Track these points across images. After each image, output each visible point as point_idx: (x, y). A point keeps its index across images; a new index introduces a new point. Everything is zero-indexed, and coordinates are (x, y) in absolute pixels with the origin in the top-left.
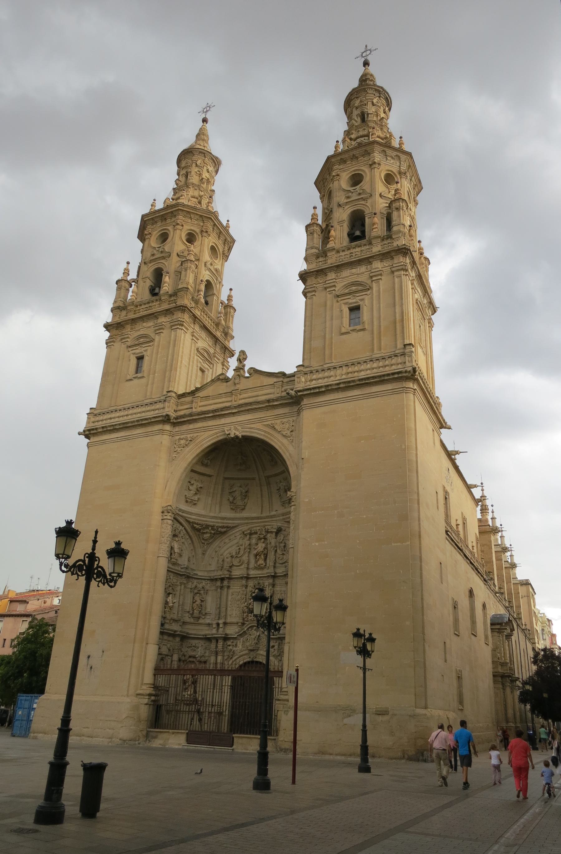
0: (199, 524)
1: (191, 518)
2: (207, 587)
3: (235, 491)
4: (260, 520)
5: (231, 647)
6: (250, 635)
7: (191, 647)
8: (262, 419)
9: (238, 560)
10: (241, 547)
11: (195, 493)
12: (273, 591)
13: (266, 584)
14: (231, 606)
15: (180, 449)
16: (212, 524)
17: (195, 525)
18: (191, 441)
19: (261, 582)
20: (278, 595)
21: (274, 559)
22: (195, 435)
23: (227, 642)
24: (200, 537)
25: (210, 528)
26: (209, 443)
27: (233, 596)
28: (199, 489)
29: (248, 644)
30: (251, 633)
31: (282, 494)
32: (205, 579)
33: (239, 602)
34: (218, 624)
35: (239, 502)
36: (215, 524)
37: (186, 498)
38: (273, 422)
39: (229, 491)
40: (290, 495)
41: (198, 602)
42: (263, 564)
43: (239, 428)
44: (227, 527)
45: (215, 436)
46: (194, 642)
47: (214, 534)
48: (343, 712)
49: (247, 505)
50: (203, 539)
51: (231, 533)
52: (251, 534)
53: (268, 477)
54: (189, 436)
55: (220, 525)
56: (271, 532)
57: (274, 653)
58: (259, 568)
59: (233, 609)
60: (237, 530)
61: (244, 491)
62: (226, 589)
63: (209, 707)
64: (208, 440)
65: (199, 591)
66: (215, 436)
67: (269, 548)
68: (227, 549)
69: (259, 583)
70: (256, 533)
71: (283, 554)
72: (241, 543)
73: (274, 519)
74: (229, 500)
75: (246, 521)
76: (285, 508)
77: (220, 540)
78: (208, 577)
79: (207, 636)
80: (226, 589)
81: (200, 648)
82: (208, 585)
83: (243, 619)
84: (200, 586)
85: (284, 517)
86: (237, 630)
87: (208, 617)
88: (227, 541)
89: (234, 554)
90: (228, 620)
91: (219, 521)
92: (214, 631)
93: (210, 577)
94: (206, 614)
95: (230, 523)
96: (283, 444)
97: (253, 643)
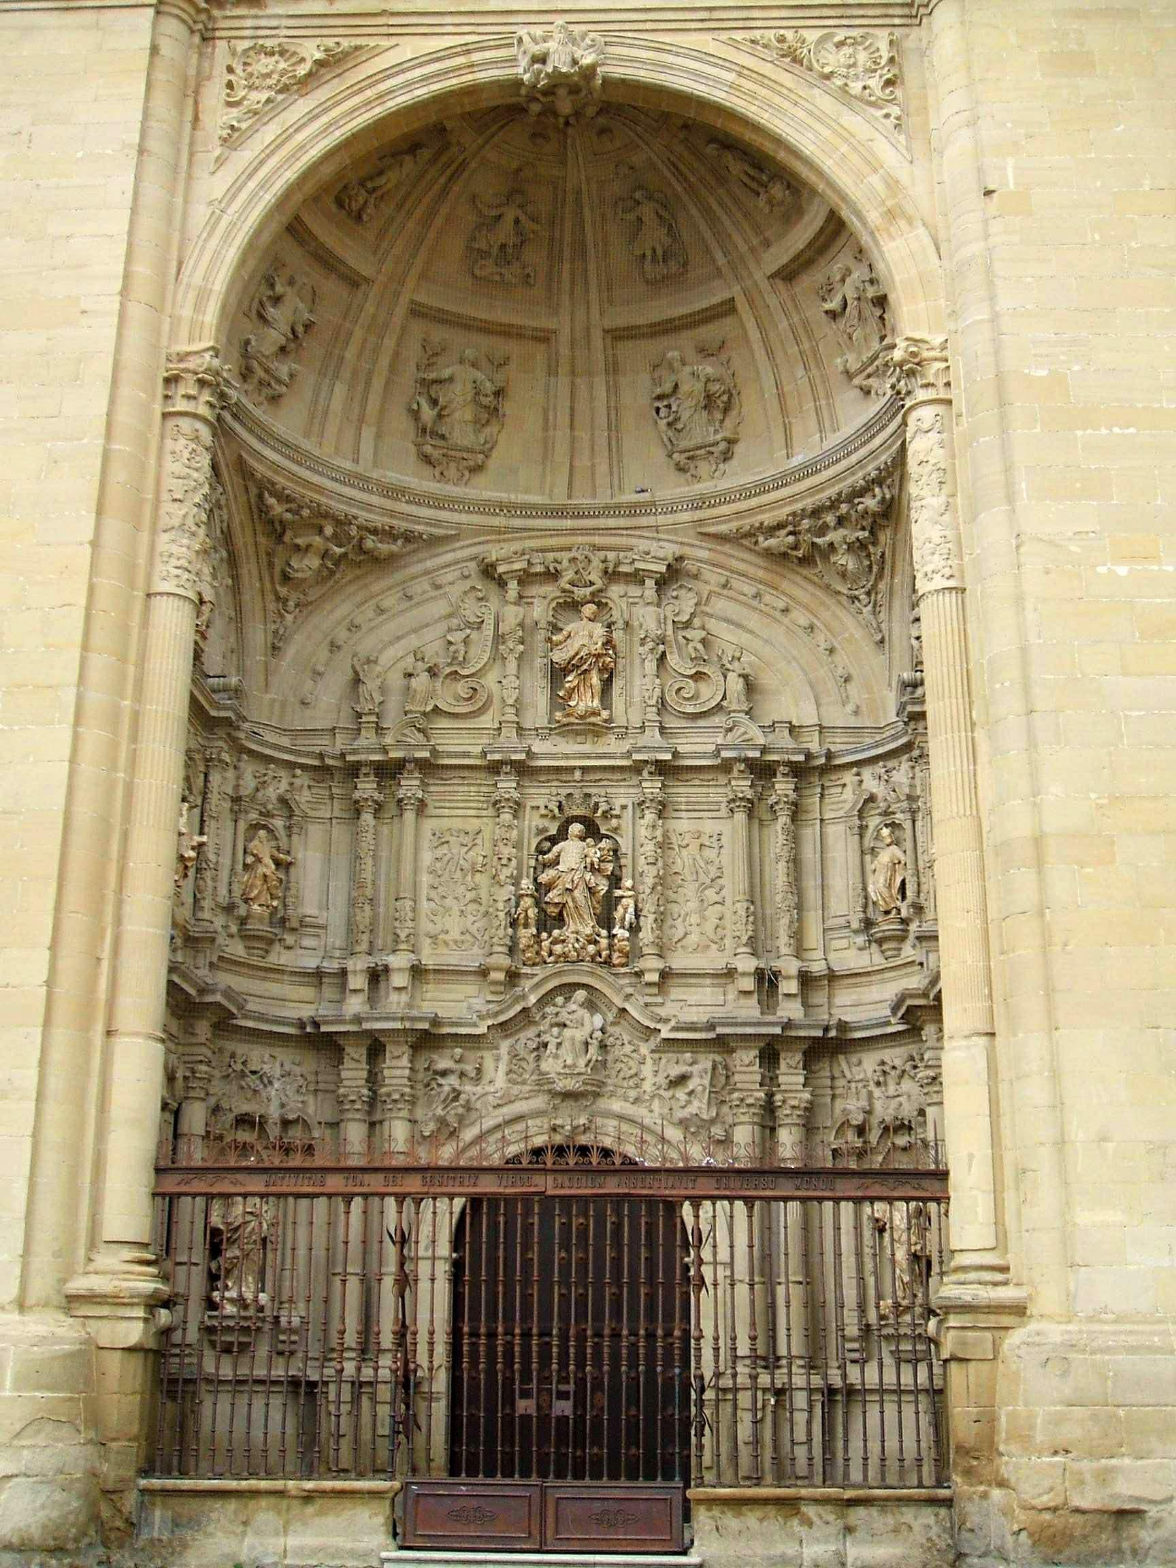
0: (288, 499)
1: (261, 458)
2: (303, 798)
3: (451, 379)
4: (569, 523)
5: (453, 1080)
6: (565, 1025)
7: (243, 1075)
8: (716, 15)
9: (461, 688)
10: (475, 635)
11: (283, 341)
12: (666, 835)
14: (433, 894)
15: (263, 96)
16: (340, 508)
17: (272, 501)
19: (592, 791)
20: (684, 852)
21: (657, 692)
23: (435, 1057)
24: (271, 565)
25: (329, 531)
26: (422, 92)
27: (444, 849)
28: (300, 329)
29: (548, 1065)
30: (564, 1017)
31: (685, 416)
32: (291, 765)
33: (482, 880)
34: (377, 976)
35: (461, 430)
36: (354, 511)
37: (245, 355)
41: (268, 867)
42: (596, 713)
44: (408, 537)
45: (461, 60)
46: (257, 1056)
47: (338, 561)
49: (495, 454)
50: (286, 578)
51: (416, 569)
52: (526, 578)
53: (618, 335)
55: (379, 520)
56: (637, 578)
57: (693, 1109)
58: (592, 729)
59: (448, 910)
60: (449, 557)
61: (489, 387)
62: (409, 816)
64: (417, 73)
65: (268, 814)
66: (461, 60)
67: (621, 647)
69: (588, 795)
70: (552, 575)
71: (698, 676)
72: (470, 610)
73: (644, 521)
74: (415, 414)
76: (697, 478)
77: (358, 599)
78: (308, 755)
79: (323, 1029)
80: (409, 816)
81: (277, 1085)
83: (512, 950)
84: (271, 793)
85: (699, 514)
86: (479, 1004)
87: (307, 942)
88: (389, 601)
89: (441, 661)
90: (428, 958)
91: (375, 500)
92: (355, 1005)
93: (321, 756)
94: (302, 924)
97: (582, 1062)
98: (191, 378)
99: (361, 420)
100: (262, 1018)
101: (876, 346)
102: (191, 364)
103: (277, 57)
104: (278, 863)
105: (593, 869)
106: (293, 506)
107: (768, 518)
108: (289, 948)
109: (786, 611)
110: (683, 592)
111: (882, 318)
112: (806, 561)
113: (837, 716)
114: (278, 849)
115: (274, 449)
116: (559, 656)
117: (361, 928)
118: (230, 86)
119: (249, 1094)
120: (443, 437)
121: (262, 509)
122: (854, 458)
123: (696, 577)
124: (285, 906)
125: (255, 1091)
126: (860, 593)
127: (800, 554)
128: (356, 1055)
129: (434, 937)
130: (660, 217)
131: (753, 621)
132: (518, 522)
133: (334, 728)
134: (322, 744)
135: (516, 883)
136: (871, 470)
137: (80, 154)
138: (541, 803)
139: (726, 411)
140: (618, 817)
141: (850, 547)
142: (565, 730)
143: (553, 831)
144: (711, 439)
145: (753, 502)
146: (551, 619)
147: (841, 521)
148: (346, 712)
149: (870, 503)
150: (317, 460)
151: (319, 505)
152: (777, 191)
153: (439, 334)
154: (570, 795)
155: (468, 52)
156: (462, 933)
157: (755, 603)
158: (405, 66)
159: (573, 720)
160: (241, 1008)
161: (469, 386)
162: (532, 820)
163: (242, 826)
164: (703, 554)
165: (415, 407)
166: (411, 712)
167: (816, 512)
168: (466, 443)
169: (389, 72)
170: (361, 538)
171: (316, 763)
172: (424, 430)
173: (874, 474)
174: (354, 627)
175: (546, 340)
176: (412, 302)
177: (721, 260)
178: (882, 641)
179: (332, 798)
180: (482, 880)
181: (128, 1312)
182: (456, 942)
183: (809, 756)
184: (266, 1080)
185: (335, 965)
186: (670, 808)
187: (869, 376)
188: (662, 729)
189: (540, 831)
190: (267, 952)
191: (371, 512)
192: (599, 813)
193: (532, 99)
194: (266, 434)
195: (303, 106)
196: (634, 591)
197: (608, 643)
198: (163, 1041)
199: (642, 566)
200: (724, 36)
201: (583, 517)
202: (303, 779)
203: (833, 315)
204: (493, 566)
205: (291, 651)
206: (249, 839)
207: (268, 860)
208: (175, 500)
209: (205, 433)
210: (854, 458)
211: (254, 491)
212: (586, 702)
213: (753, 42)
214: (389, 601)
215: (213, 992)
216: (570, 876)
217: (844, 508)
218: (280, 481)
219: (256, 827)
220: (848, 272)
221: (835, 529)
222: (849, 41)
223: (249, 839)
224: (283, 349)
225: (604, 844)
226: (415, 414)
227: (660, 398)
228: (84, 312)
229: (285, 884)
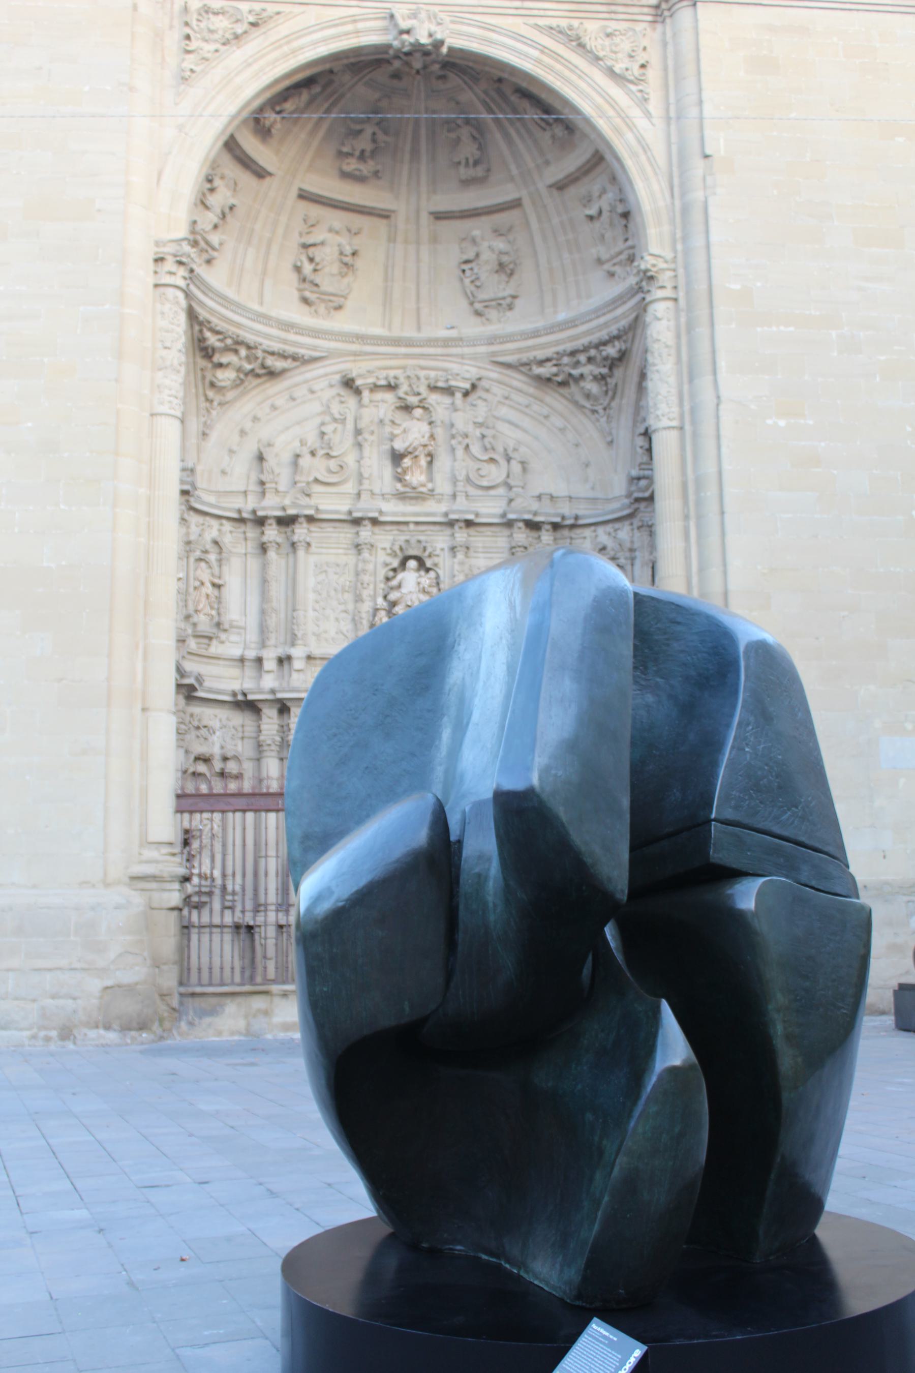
0: (218, 333)
4: (403, 350)
7: (198, 728)
9: (333, 464)
10: (340, 427)
11: (215, 220)
13: (439, 545)
16: (250, 338)
17: (208, 334)
18: (254, 25)
19: (422, 538)
22: (271, 8)
24: (204, 378)
25: (243, 352)
26: (323, 50)
27: (323, 577)
28: (227, 210)
31: (484, 276)
34: (283, 661)
36: (260, 340)
38: (575, 23)
39: (303, 240)
40: (654, 266)
41: (208, 589)
42: (424, 485)
43: (447, 19)
44: (294, 358)
45: (350, 28)
48: (905, 898)
50: (212, 385)
51: (299, 379)
52: (375, 388)
54: (244, 7)
55: (276, 346)
56: (449, 391)
60: (321, 371)
61: (348, 250)
62: (301, 553)
63: (266, 911)
64: (319, 35)
65: (206, 552)
66: (350, 28)
68: (287, 428)
69: (419, 542)
70: (391, 387)
71: (492, 460)
72: (336, 409)
75: (355, 347)
78: (230, 510)
81: (218, 733)
82: (229, 535)
87: (234, 638)
91: (274, 332)
92: (269, 682)
93: (239, 511)
94: (232, 626)
95: (304, 344)
96: (612, 102)
98: (170, 260)
99: (264, 272)
100: (210, 691)
101: (621, 245)
102: (170, 249)
103: (220, 17)
104: (214, 585)
105: (424, 591)
106: (220, 337)
107: (541, 354)
108: (222, 642)
109: (546, 417)
110: (479, 402)
111: (626, 226)
112: (563, 384)
113: (582, 490)
114: (213, 575)
115: (211, 299)
116: (399, 446)
117: (271, 629)
118: (188, 37)
119: (202, 739)
120: (317, 285)
121: (202, 340)
122: (602, 320)
123: (487, 391)
124: (219, 614)
125: (206, 739)
126: (599, 408)
127: (559, 379)
128: (270, 715)
129: (317, 635)
130: (474, 138)
131: (526, 422)
132: (368, 349)
133: (245, 492)
134: (237, 503)
135: (374, 598)
136: (614, 329)
137: (87, 88)
138: (387, 545)
139: (511, 274)
140: (438, 556)
141: (595, 378)
142: (401, 497)
143: (395, 563)
144: (501, 295)
145: (530, 342)
146: (391, 418)
147: (590, 360)
148: (254, 477)
149: (611, 351)
150: (238, 305)
151: (238, 336)
152: (559, 131)
153: (315, 211)
154: (407, 541)
155: (355, 21)
156: (337, 633)
157: (527, 410)
158: (311, 29)
159: (407, 490)
160: (201, 684)
161: (336, 249)
162: (382, 557)
163: (192, 560)
164: (494, 375)
165: (299, 264)
166: (300, 482)
167: (573, 353)
168: (330, 289)
169: (302, 33)
170: (264, 358)
171: (235, 515)
172: (304, 280)
173: (615, 333)
174: (256, 419)
175: (387, 217)
176: (300, 189)
177: (515, 171)
178: (612, 442)
179: (246, 539)
180: (349, 597)
181: (168, 886)
182: (333, 639)
183: (563, 518)
184: (211, 731)
185: (251, 654)
186: (472, 550)
187: (614, 265)
188: (467, 496)
189: (386, 565)
190: (209, 645)
191: (270, 340)
192: (427, 553)
193: (397, 57)
194: (207, 289)
195: (237, 55)
196: (447, 400)
197: (432, 437)
198: (174, 713)
199: (453, 383)
200: (532, 21)
201: (413, 346)
202: (227, 526)
203: (591, 218)
204: (353, 380)
205: (214, 436)
206: (196, 569)
207: (208, 585)
208: (166, 348)
209: (181, 296)
210: (602, 320)
211: (197, 328)
212: (416, 477)
213: (551, 28)
214: (280, 401)
215: (189, 677)
216: (409, 597)
217: (593, 352)
218: (215, 321)
219: (201, 560)
220: (603, 191)
221: (585, 365)
222: (617, 33)
223: (196, 569)
224: (216, 227)
225: (432, 574)
226: (298, 269)
227: (467, 262)
228: (99, 211)
229: (219, 599)
